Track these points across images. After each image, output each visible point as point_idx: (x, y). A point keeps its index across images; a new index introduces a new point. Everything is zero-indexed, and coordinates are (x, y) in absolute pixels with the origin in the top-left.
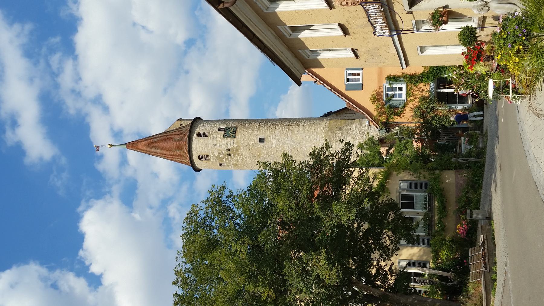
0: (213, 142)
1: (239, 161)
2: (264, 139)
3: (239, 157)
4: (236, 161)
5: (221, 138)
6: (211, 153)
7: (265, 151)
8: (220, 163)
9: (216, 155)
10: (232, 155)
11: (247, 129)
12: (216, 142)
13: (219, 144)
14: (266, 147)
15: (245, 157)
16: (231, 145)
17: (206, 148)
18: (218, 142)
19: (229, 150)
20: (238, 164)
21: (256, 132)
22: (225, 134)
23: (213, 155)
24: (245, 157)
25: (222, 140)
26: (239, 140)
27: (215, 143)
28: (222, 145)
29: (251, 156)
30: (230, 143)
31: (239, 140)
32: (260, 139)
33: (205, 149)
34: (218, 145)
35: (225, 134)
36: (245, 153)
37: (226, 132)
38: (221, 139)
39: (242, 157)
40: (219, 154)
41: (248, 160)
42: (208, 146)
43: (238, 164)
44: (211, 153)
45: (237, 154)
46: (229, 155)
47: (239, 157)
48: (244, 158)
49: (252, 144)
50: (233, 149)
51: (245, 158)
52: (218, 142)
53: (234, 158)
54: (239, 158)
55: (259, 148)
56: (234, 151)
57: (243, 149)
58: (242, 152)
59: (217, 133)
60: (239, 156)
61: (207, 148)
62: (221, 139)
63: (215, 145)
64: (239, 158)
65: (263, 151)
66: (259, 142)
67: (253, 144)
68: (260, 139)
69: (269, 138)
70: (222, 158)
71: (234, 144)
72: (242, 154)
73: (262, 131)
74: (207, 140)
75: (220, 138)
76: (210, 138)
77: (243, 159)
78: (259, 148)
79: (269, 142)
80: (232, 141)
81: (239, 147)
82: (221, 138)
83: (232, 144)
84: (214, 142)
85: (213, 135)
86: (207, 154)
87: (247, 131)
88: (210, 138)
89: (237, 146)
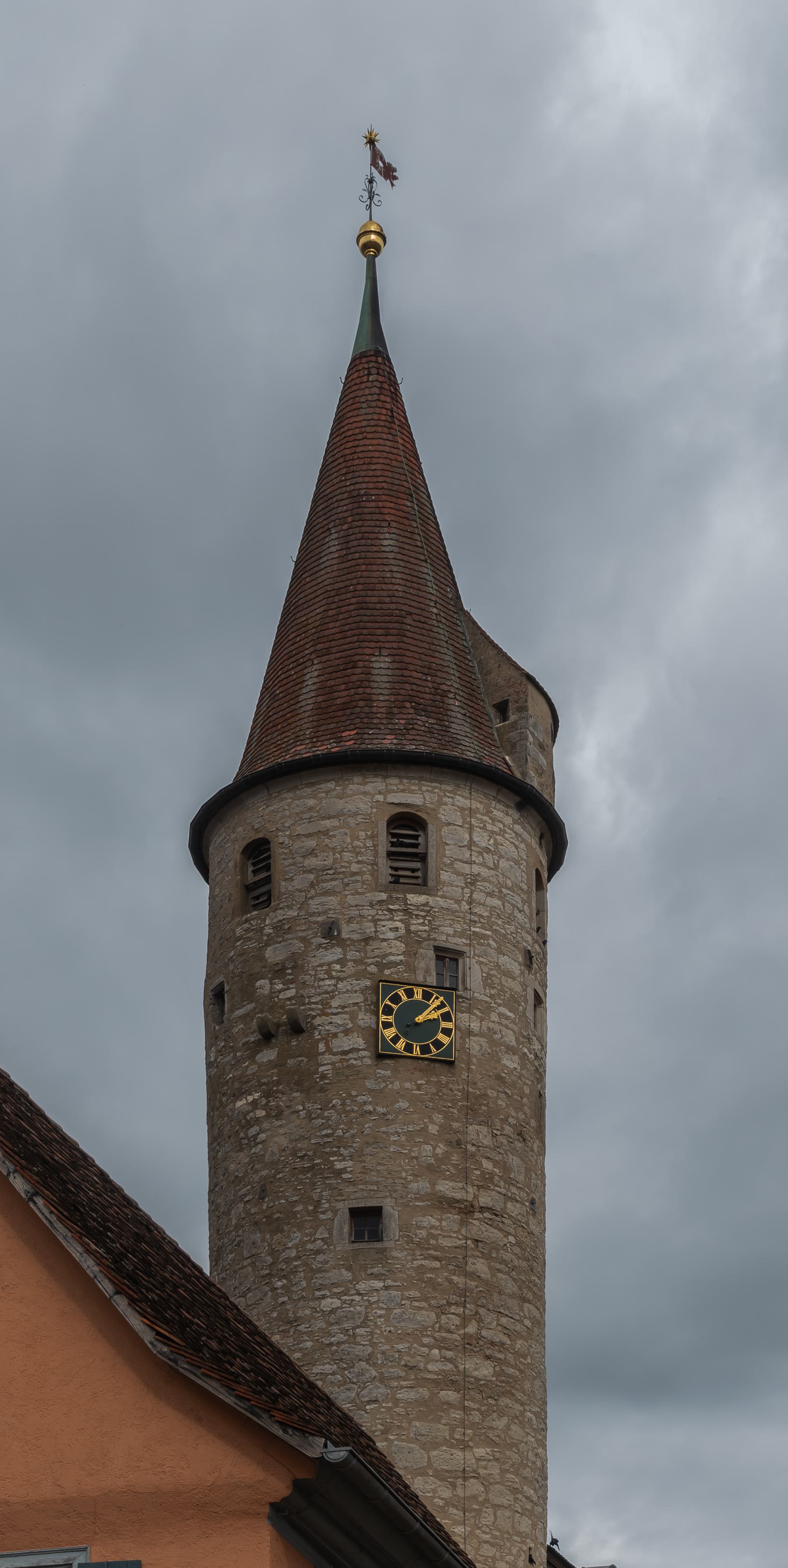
0: (350, 920)
1: (239, 1104)
2: (376, 1235)
3: (256, 1095)
4: (236, 1085)
5: (381, 966)
6: (280, 915)
7: (293, 1254)
8: (227, 988)
9: (269, 952)
10: (268, 1055)
11: (445, 1128)
12: (355, 937)
13: (338, 962)
14: (321, 1258)
15: (263, 1136)
16: (335, 1035)
17: (312, 876)
18: (352, 955)
19: (296, 1028)
20: (224, 1099)
21: (422, 1185)
22: (410, 993)
23: (268, 930)
24: (263, 1136)
25: (358, 976)
26: (369, 1084)
27: (344, 935)
28: (331, 977)
29: (265, 1173)
30: (347, 1032)
31: (369, 1084)
32: (376, 1212)
33: (310, 871)
34: (336, 953)
35: (410, 993)
36: (282, 1131)
37: (418, 995)
38: (373, 969)
39: (261, 1113)
40: (278, 971)
41: (241, 1155)
42: (326, 893)
43: (224, 1099)
44: (280, 915)
45: (278, 1083)
46: (267, 1036)
47: (256, 1095)
48: (253, 1131)
49: (339, 1166)
50: (313, 1055)
51: (255, 1137)
52: (352, 955)
53: (253, 1069)
54: (250, 1099)
55: (309, 1213)
56: (291, 1062)
57: (310, 1117)
58: (286, 1112)
59: (411, 940)
60: (267, 1095)
61: (312, 885)
62: (373, 969)
63: (330, 931)
64: (250, 1099)
65: (297, 1237)
66: (350, 1209)
67: (339, 1172)
68: (376, 1212)
69: (375, 1270)
70: (248, 993)
71: (336, 1058)
72: (278, 1116)
73: (430, 1220)
74: (367, 877)
75: (377, 964)
76: (384, 896)
77: (249, 1125)
78: (315, 1211)
79: (349, 1268)
80: (360, 1042)
81: (322, 1090)
82: (381, 966)
83: (344, 1043)
84: (354, 926)
85: (399, 916)
86: (275, 893)
87: (433, 1129)
88: (384, 896)
89: (323, 1076)
